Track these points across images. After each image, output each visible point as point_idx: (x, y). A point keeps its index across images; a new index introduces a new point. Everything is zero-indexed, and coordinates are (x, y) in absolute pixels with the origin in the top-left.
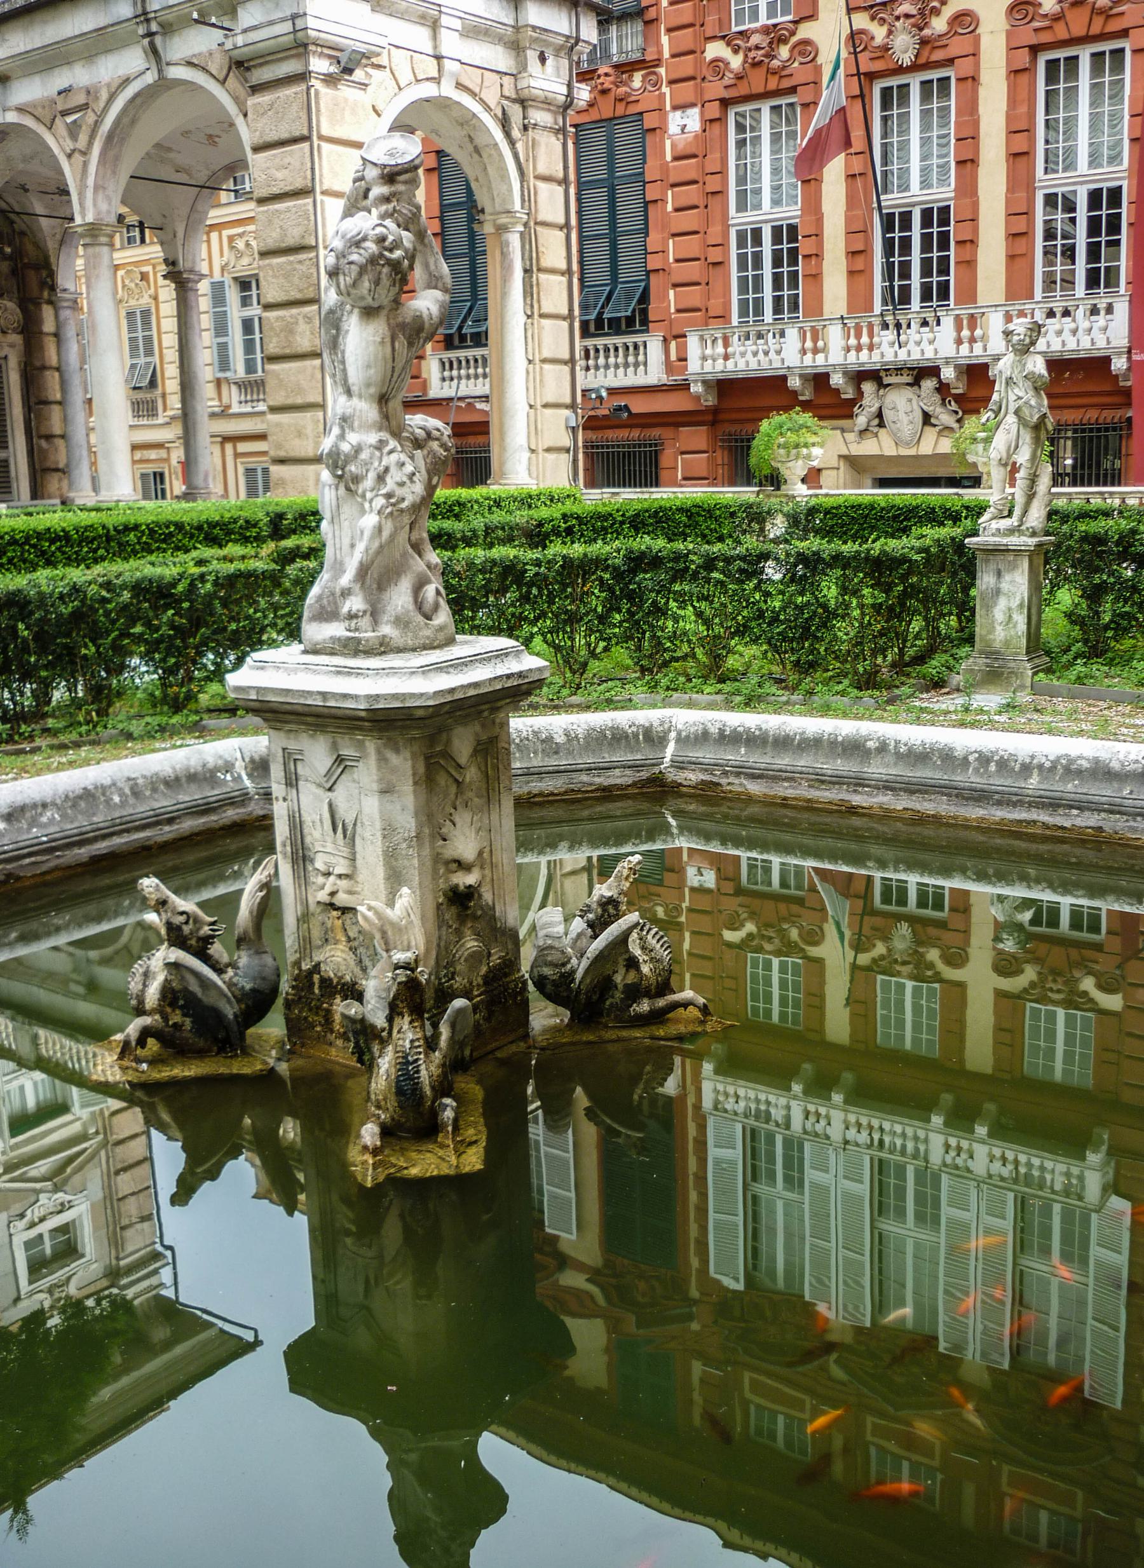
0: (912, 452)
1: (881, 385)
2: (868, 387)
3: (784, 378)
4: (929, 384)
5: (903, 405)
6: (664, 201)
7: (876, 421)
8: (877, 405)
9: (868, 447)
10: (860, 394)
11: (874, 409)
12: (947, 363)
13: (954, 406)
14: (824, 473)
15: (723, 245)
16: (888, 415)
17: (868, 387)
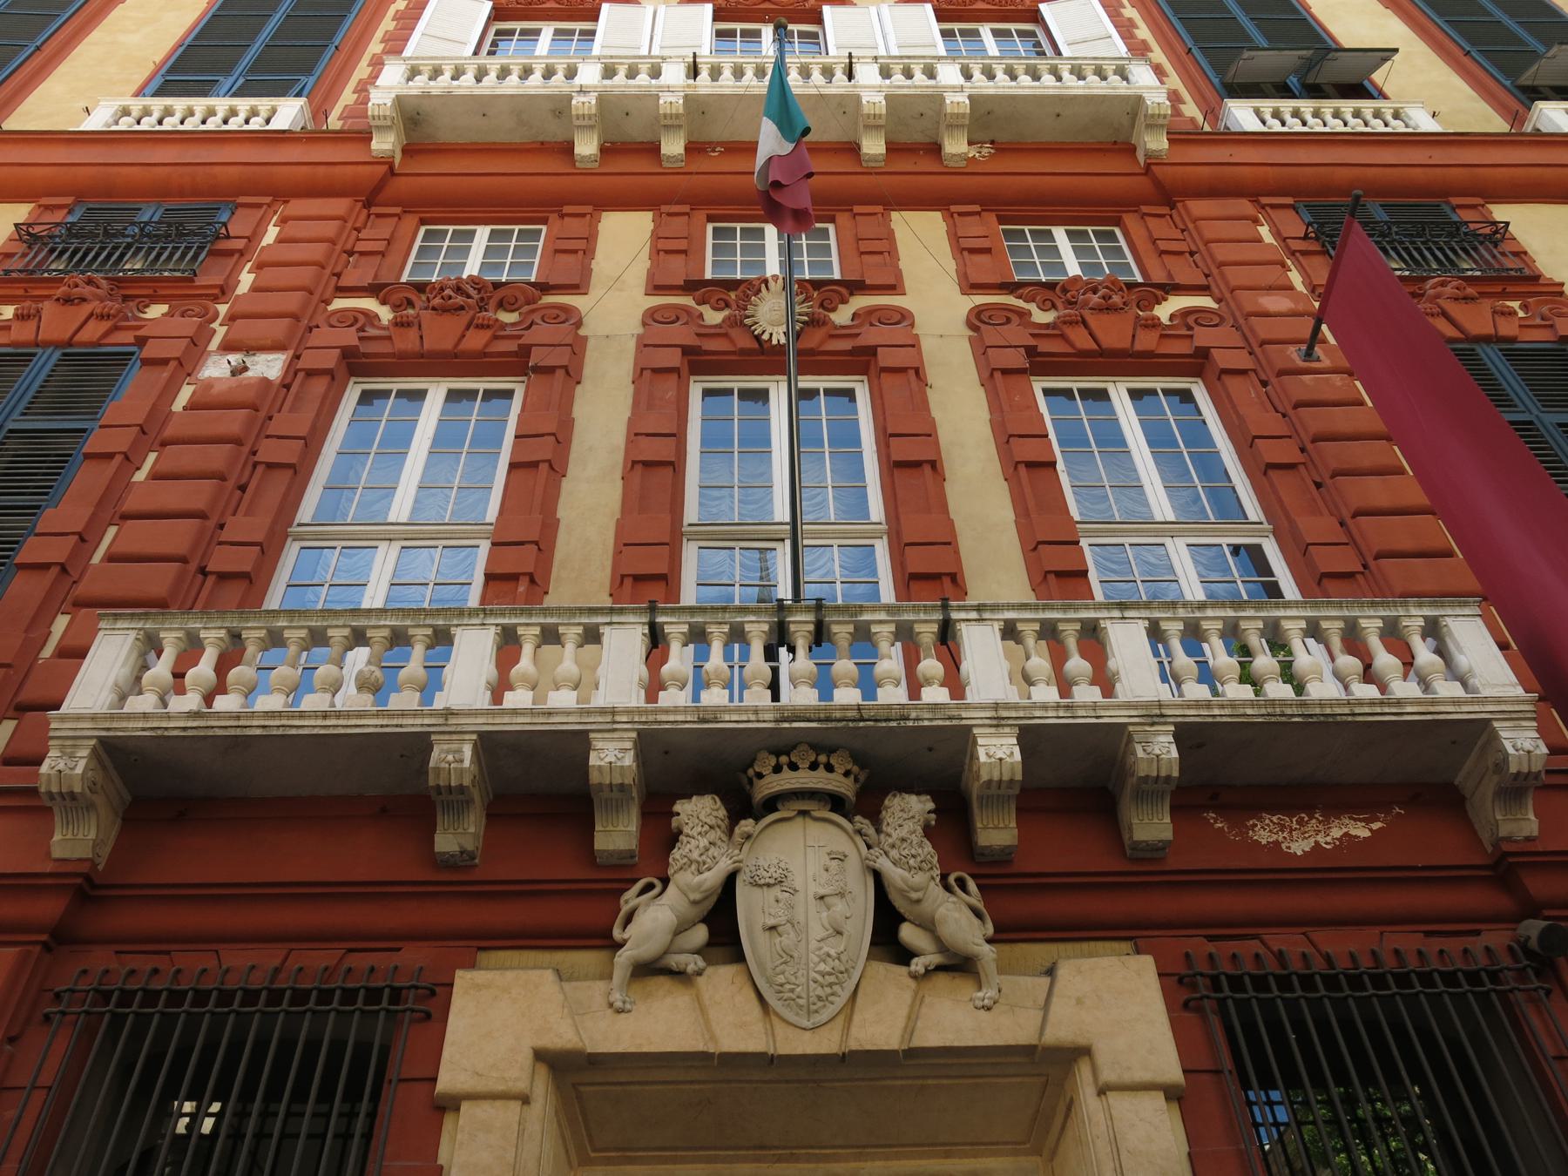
0: (825, 1043)
1: (742, 806)
2: (698, 814)
3: (421, 744)
4: (908, 812)
5: (807, 876)
6: (131, 461)
7: (700, 934)
8: (724, 866)
9: (660, 1024)
10: (662, 837)
11: (712, 878)
12: (998, 723)
13: (975, 896)
14: (465, 1107)
16: (751, 908)
17: (698, 814)
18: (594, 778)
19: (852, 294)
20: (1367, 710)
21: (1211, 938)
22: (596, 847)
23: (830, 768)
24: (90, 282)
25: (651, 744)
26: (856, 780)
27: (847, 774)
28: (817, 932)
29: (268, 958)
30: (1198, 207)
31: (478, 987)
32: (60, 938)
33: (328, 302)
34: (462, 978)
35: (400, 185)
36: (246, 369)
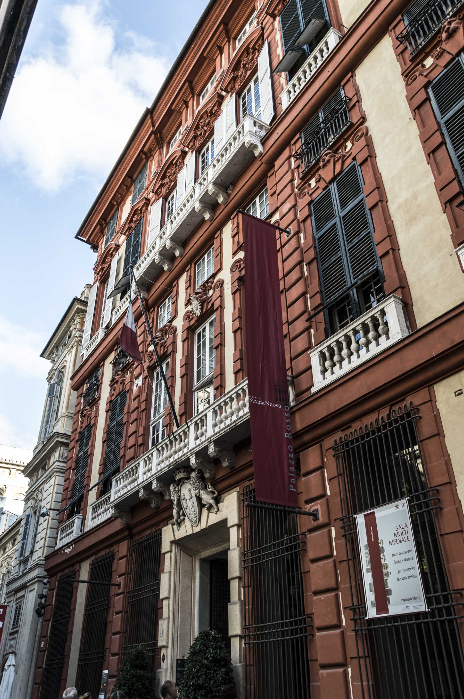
15: (145, 435)
18: (155, 490)
19: (214, 279)
20: (238, 422)
21: (249, 480)
22: (166, 499)
23: (181, 473)
24: (118, 375)
25: (159, 479)
26: (187, 472)
27: (184, 472)
28: (191, 507)
29: (148, 532)
30: (277, 164)
31: (164, 531)
32: (131, 536)
33: (147, 351)
34: (163, 529)
35: (150, 301)
36: (137, 384)
